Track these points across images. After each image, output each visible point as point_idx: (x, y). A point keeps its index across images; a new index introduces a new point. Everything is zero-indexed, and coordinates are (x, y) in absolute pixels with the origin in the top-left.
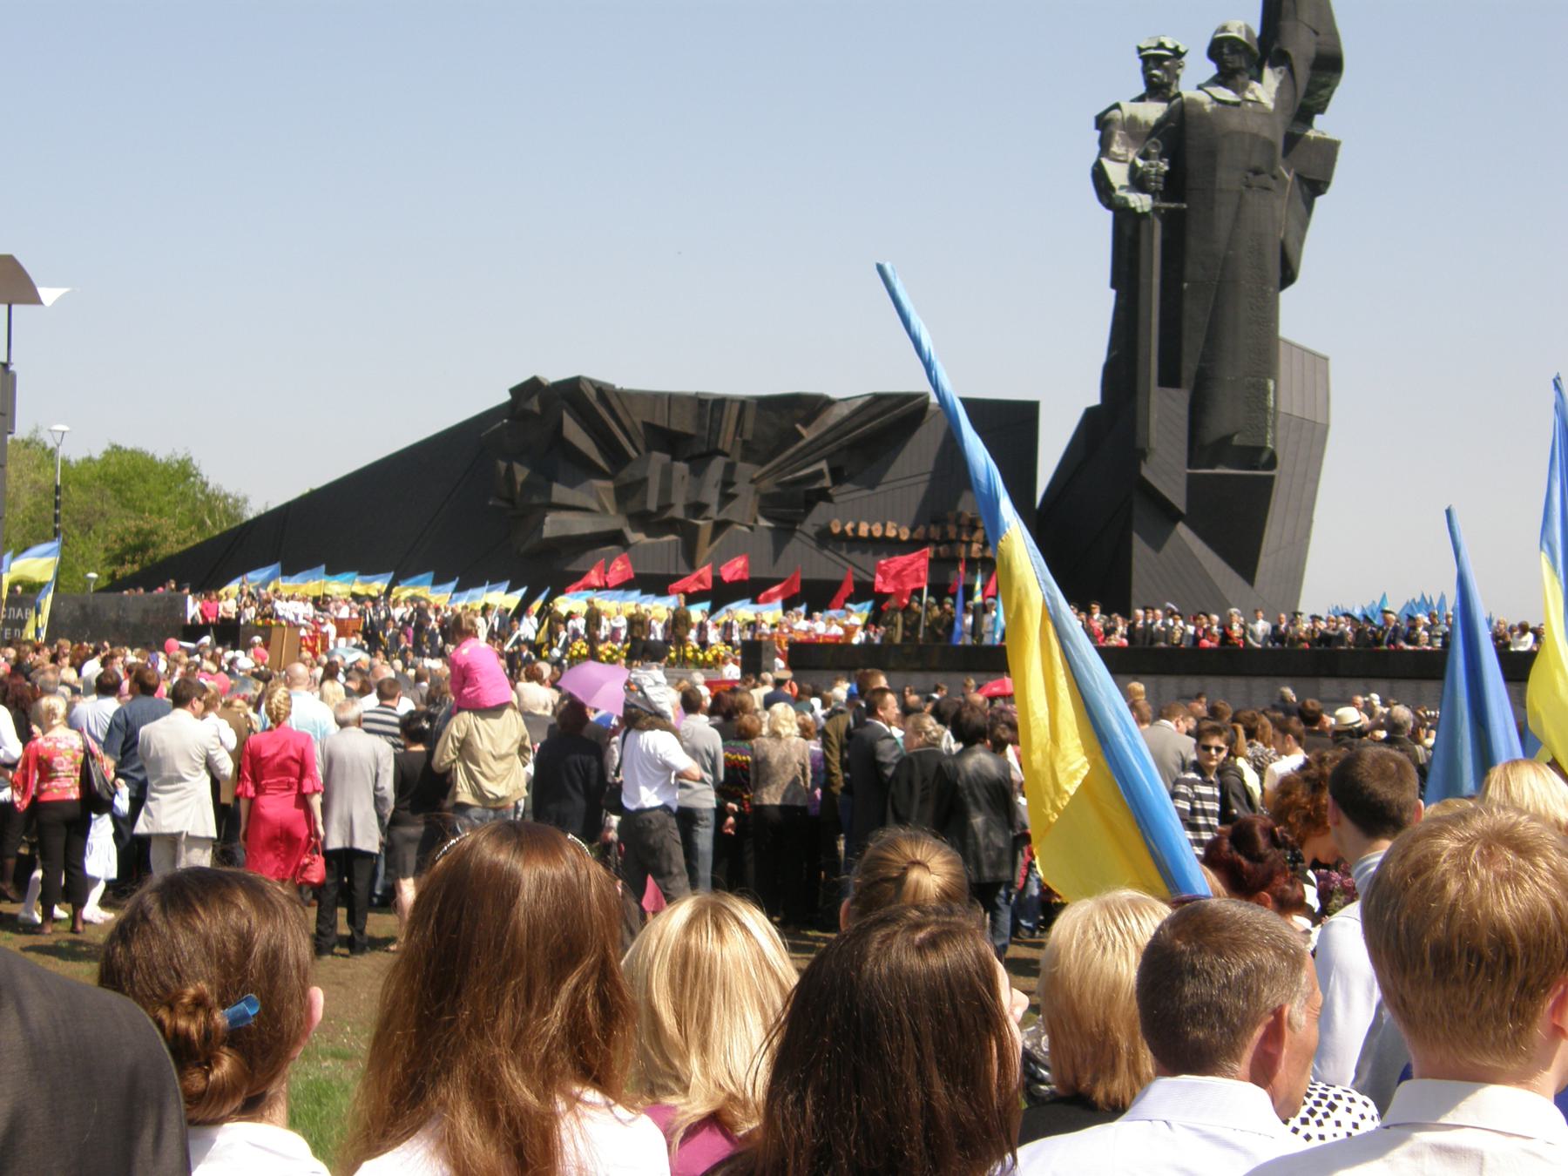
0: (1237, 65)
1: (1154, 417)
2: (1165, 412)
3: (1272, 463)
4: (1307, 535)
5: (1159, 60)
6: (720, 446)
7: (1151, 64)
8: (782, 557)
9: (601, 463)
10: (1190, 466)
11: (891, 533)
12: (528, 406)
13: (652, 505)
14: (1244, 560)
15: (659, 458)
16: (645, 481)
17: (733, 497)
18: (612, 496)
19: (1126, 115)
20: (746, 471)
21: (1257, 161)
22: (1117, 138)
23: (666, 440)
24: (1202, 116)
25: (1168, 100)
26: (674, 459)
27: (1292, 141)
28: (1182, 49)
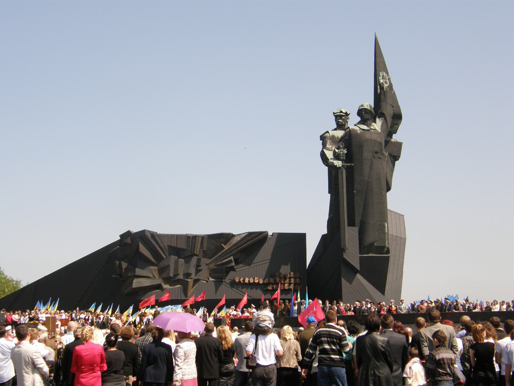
1: (347, 236)
2: (350, 236)
3: (388, 252)
5: (341, 117)
6: (195, 253)
7: (338, 118)
8: (218, 292)
9: (153, 260)
10: (360, 254)
11: (257, 281)
12: (126, 241)
13: (171, 275)
14: (381, 287)
15: (174, 258)
16: (169, 266)
17: (200, 270)
18: (157, 272)
19: (331, 135)
20: (205, 261)
21: (376, 149)
23: (176, 251)
24: (357, 134)
25: (345, 130)
26: (178, 258)
27: (387, 142)
28: (348, 113)
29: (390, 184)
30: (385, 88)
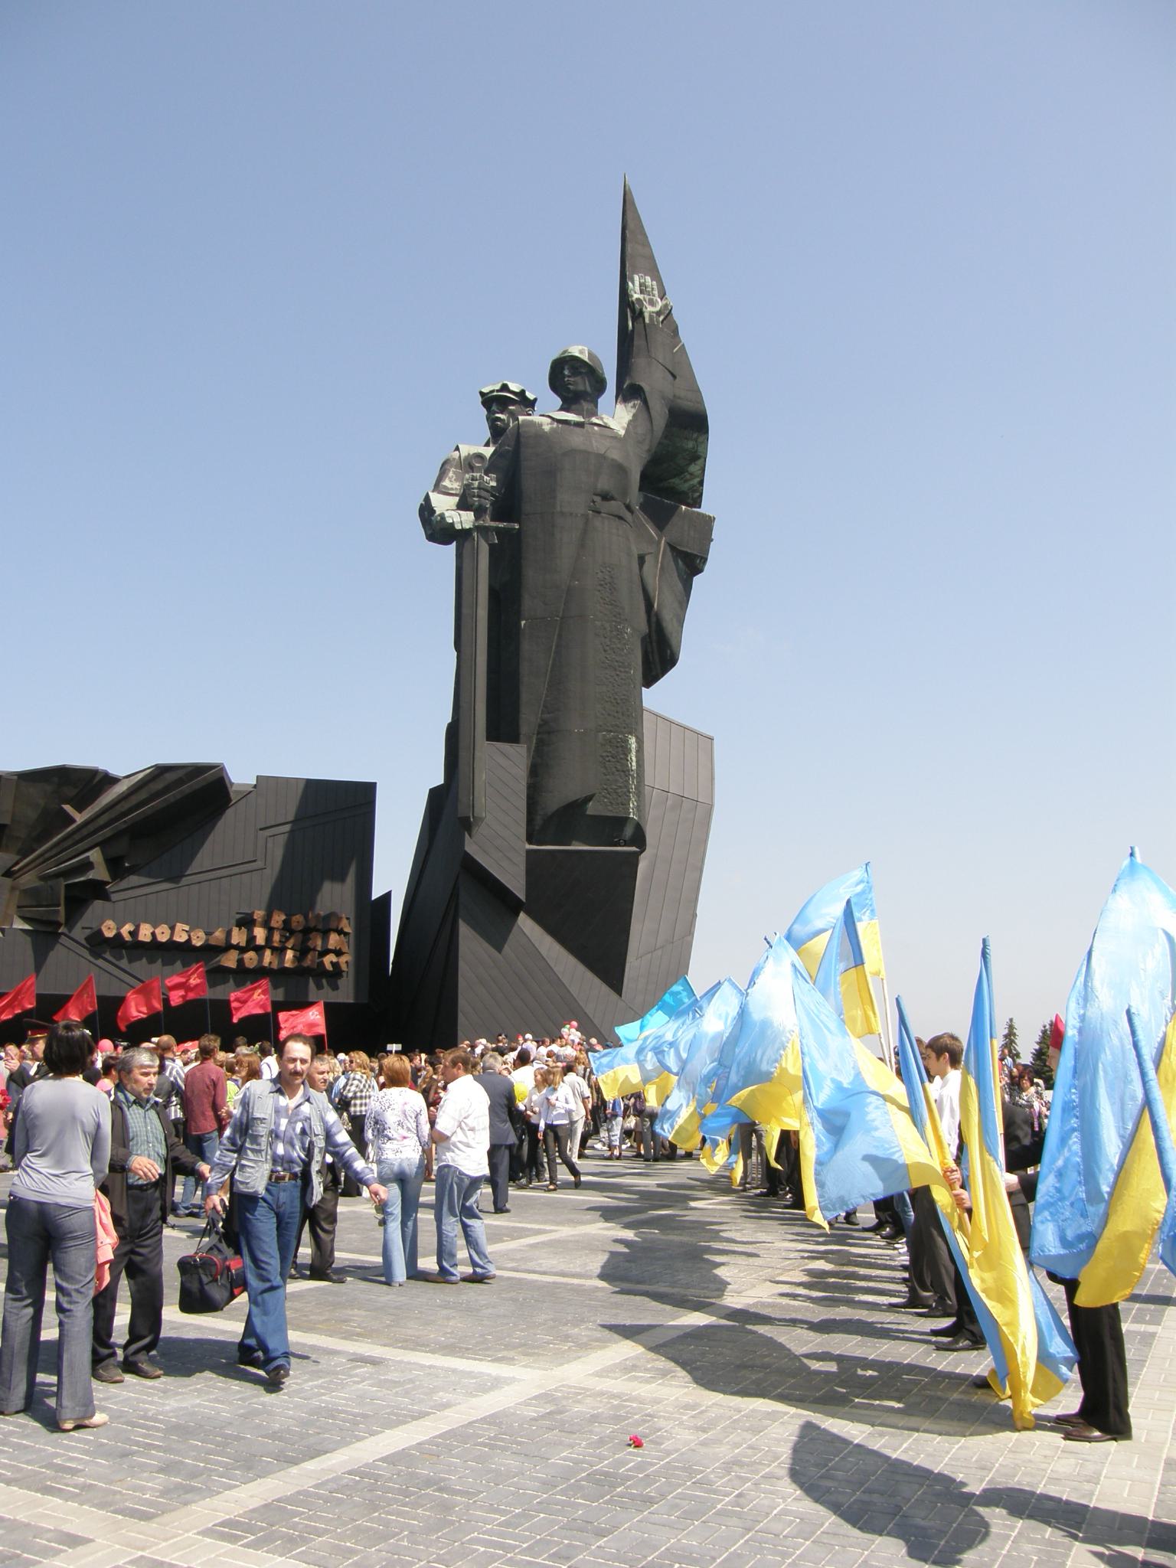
0: (581, 388)
4: (690, 932)
7: (494, 408)
8: (43, 971)
10: (530, 839)
11: (181, 937)
21: (604, 483)
22: (451, 474)
28: (530, 395)
29: (673, 642)
30: (646, 315)
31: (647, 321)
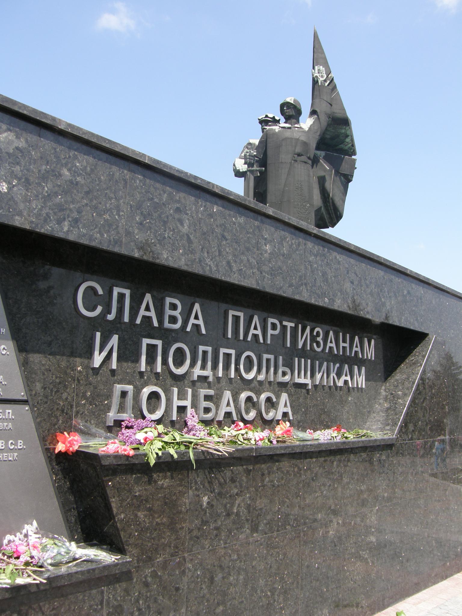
0: (291, 114)
21: (298, 150)
29: (340, 209)
30: (319, 82)
31: (320, 84)
